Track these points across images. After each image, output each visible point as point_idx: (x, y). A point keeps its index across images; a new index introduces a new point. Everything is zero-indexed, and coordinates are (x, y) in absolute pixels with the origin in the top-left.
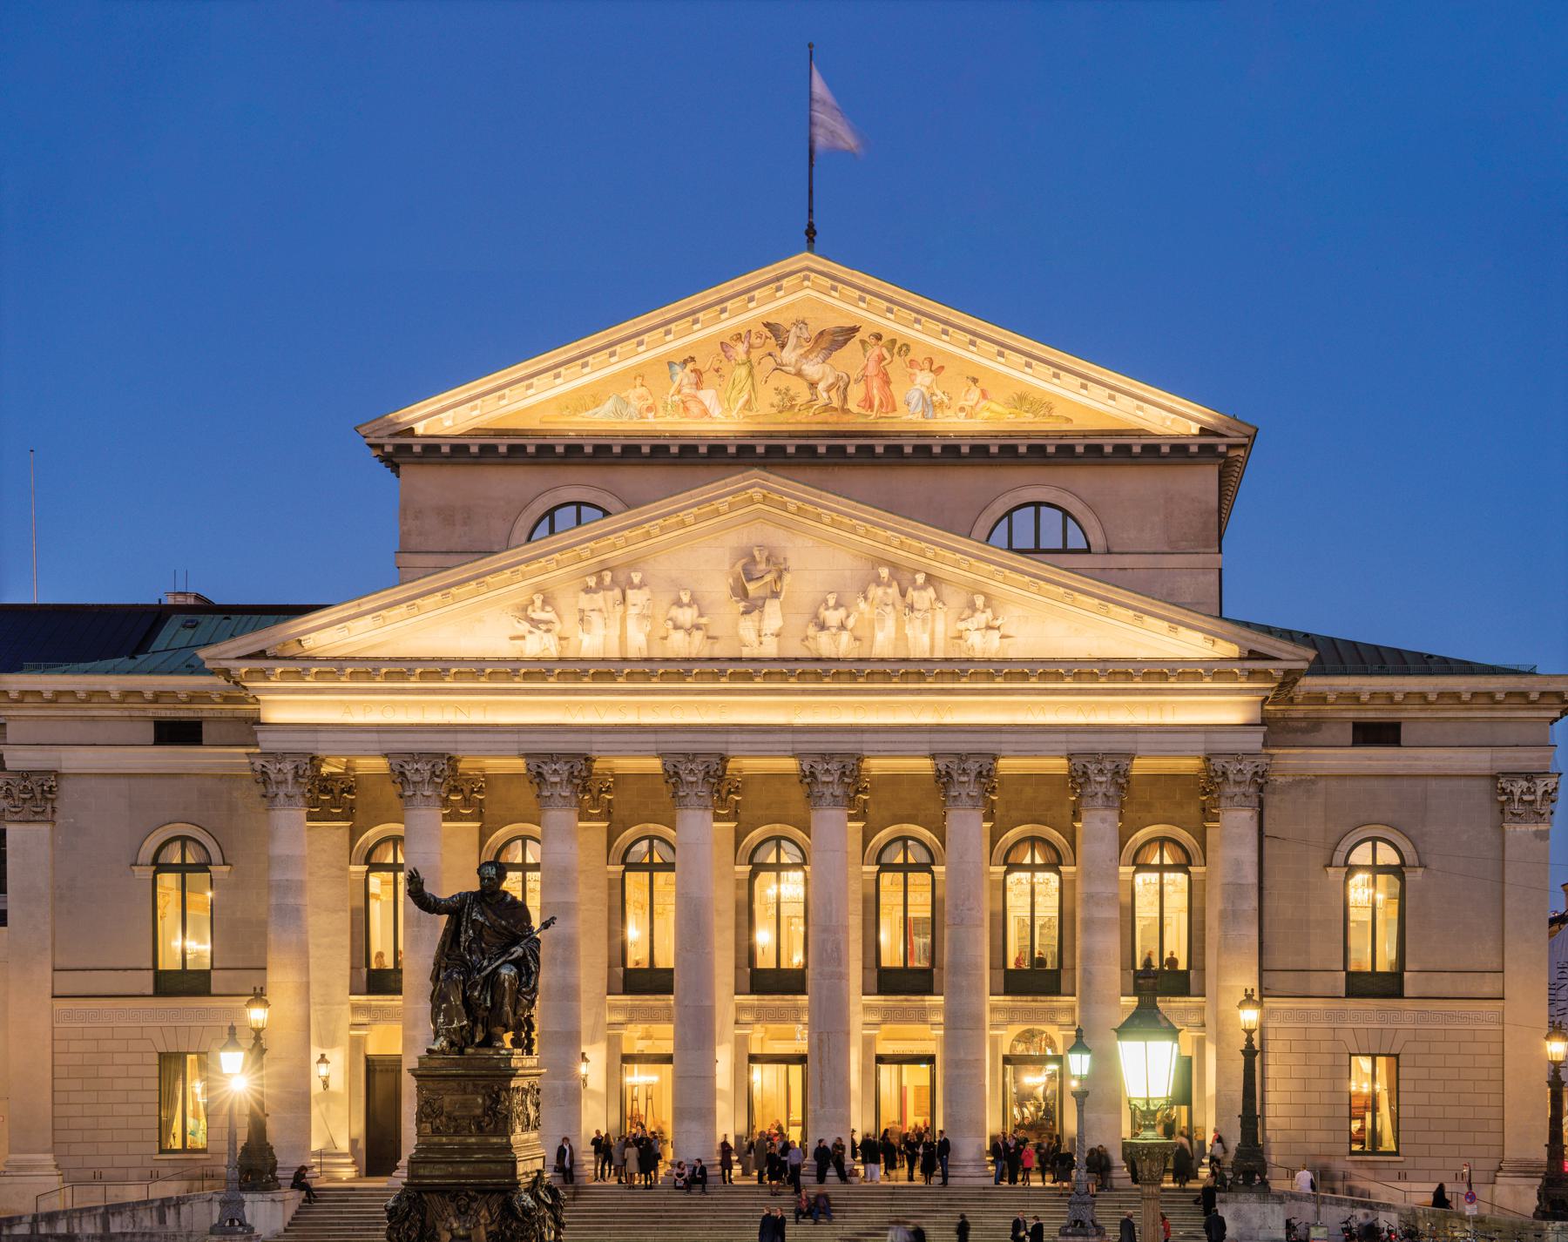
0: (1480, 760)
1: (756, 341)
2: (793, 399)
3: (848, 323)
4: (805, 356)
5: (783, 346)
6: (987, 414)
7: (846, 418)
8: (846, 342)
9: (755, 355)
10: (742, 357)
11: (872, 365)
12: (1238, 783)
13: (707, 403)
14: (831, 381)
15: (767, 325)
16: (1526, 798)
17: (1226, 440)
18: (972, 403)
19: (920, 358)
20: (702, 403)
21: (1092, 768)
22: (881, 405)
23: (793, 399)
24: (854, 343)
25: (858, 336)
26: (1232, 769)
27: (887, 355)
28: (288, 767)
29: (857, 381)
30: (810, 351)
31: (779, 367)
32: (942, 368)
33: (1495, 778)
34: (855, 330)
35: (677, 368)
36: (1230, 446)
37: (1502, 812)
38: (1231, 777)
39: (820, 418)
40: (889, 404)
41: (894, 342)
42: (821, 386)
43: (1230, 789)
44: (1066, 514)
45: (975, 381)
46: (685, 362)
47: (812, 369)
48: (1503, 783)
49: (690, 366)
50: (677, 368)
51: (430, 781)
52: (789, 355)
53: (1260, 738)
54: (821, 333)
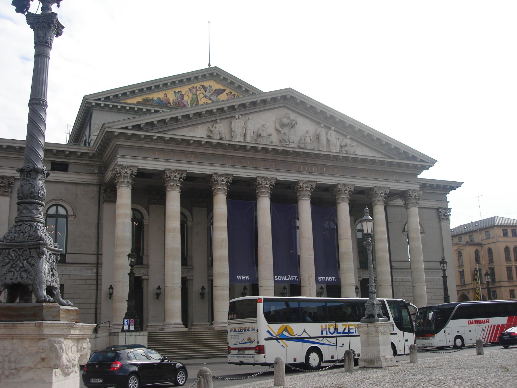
1: (198, 89)
3: (222, 88)
5: (206, 91)
8: (222, 93)
9: (198, 93)
15: (201, 85)
24: (224, 93)
25: (226, 92)
28: (129, 172)
30: (213, 94)
31: (205, 96)
33: (438, 209)
37: (439, 218)
46: (179, 92)
47: (213, 98)
52: (207, 94)
53: (419, 186)
54: (216, 90)
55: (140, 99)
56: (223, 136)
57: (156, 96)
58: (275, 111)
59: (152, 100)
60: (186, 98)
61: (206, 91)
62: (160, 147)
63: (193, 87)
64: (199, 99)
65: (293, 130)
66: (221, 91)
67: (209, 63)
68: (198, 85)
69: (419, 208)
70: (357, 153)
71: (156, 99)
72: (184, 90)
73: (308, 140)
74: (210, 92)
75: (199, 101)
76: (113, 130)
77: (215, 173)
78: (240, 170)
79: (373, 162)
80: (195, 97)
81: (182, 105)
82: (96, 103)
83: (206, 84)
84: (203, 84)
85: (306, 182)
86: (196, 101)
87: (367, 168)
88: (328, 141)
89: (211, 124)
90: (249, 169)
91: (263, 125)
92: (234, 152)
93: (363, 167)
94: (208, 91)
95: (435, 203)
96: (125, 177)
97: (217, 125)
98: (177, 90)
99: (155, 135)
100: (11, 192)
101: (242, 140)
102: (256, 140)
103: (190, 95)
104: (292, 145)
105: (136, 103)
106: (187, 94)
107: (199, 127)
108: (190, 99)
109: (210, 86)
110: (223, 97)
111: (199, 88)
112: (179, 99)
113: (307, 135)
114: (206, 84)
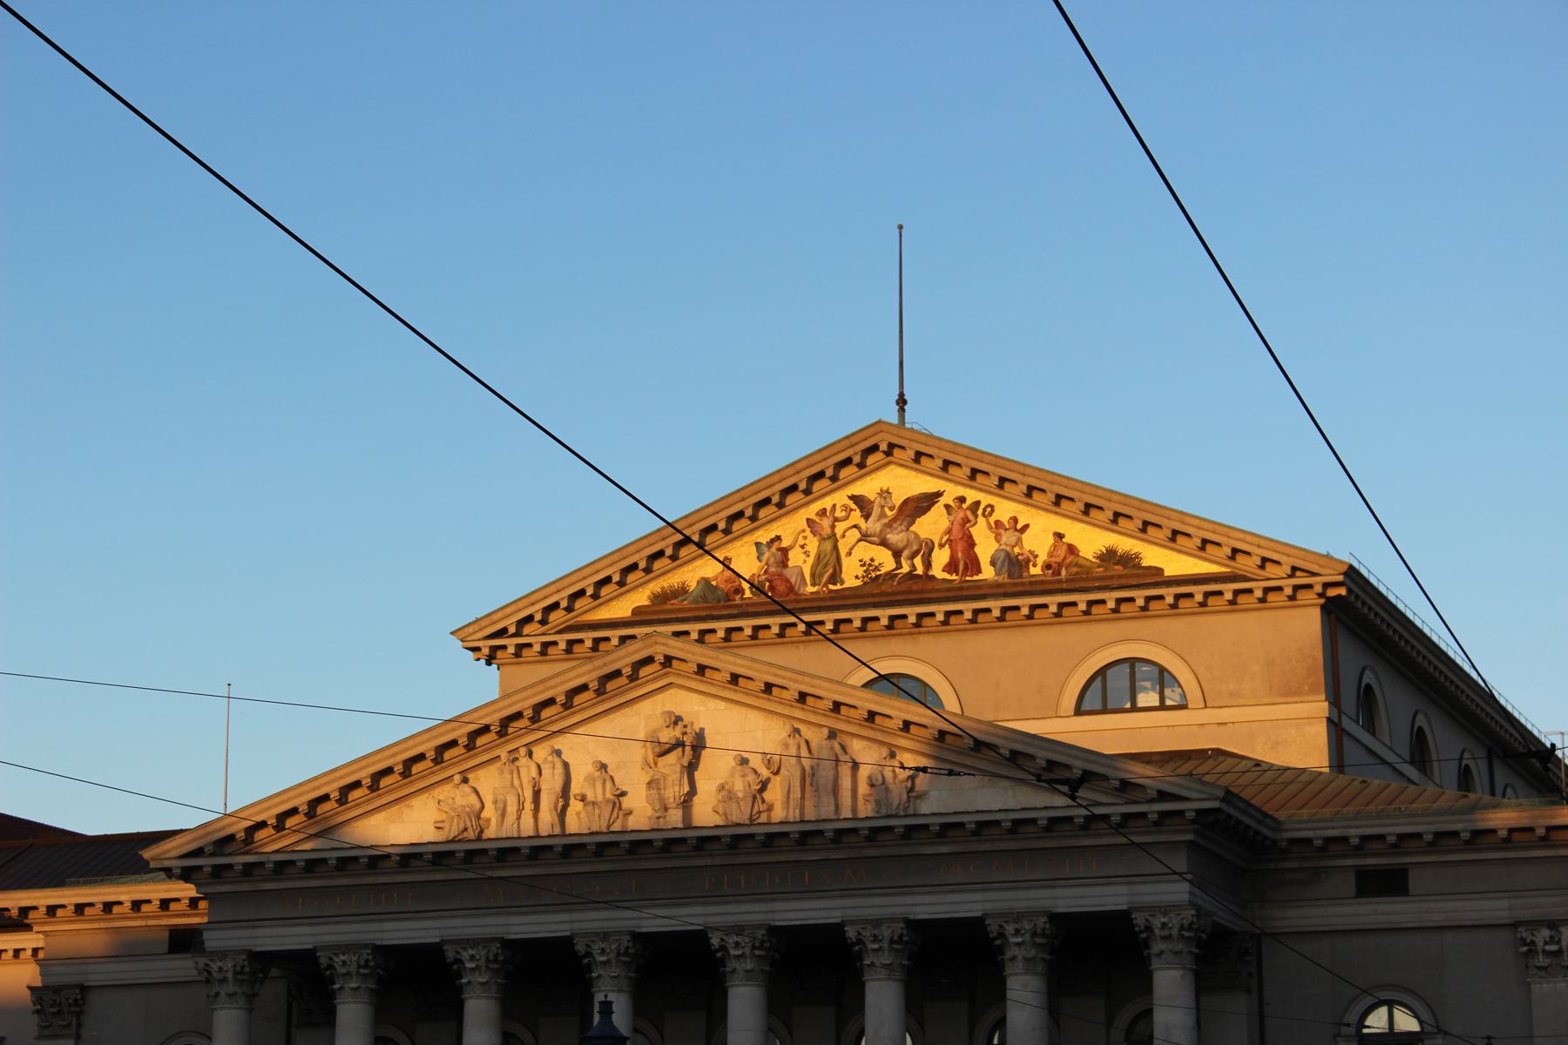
0: (1497, 909)
1: (839, 514)
2: (877, 569)
4: (889, 525)
6: (1075, 570)
7: (930, 585)
8: (929, 508)
10: (828, 531)
11: (956, 528)
13: (793, 581)
14: (915, 548)
15: (852, 498)
16: (1548, 948)
17: (1318, 579)
18: (1059, 560)
19: (1005, 520)
20: (788, 581)
21: (1010, 929)
22: (966, 568)
23: (877, 569)
24: (938, 509)
25: (943, 500)
26: (1157, 922)
27: (971, 517)
29: (941, 546)
30: (894, 520)
31: (865, 537)
32: (1026, 526)
33: (1515, 925)
34: (939, 494)
35: (765, 549)
36: (1326, 585)
38: (1157, 932)
39: (904, 587)
40: (974, 565)
41: (978, 503)
42: (906, 553)
43: (1156, 947)
44: (1162, 670)
45: (1059, 536)
46: (772, 541)
47: (895, 538)
48: (1523, 933)
49: (776, 544)
50: (765, 549)
51: (358, 974)
54: (906, 502)
55: (641, 598)
57: (698, 572)
58: (646, 705)
59: (682, 591)
60: (796, 558)
61: (867, 517)
63: (823, 512)
64: (843, 552)
66: (925, 503)
67: (901, 395)
68: (840, 498)
71: (693, 585)
72: (789, 527)
74: (883, 515)
75: (845, 561)
76: (167, 864)
78: (526, 919)
79: (949, 829)
80: (828, 546)
81: (781, 588)
82: (494, 649)
83: (868, 487)
84: (858, 489)
85: (738, 929)
86: (833, 561)
90: (555, 912)
93: (944, 849)
94: (876, 511)
95: (1504, 903)
96: (225, 980)
98: (763, 536)
100: (79, 1026)
101: (527, 827)
103: (813, 545)
105: (628, 613)
106: (801, 541)
107: (415, 802)
108: (811, 561)
109: (885, 494)
110: (932, 525)
111: (846, 508)
112: (772, 569)
114: (868, 487)
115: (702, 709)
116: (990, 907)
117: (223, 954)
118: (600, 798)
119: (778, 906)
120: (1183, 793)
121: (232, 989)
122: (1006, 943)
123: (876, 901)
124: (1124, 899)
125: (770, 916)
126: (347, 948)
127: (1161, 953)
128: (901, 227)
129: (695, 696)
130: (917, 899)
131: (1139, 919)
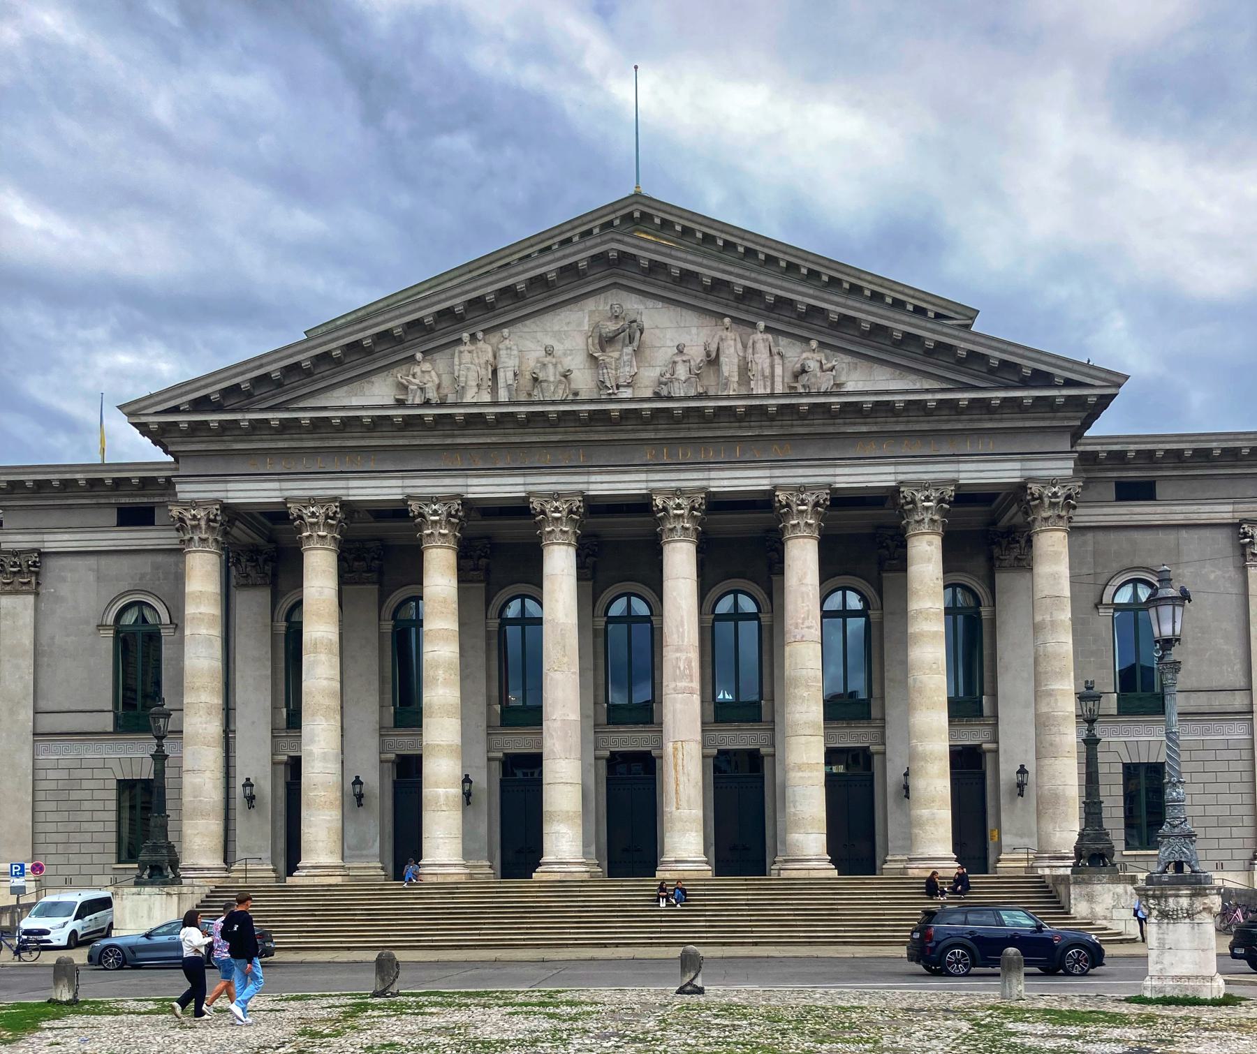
12: (1053, 505)
21: (919, 496)
26: (1047, 493)
38: (1046, 501)
53: (1071, 464)
56: (433, 395)
58: (590, 304)
62: (273, 445)
65: (629, 350)
69: (1075, 531)
70: (850, 387)
73: (682, 372)
77: (409, 497)
79: (884, 409)
85: (678, 493)
87: (874, 429)
88: (745, 370)
89: (405, 367)
91: (549, 352)
92: (463, 436)
93: (864, 429)
97: (417, 369)
99: (245, 417)
101: (487, 398)
102: (530, 395)
104: (626, 393)
107: (374, 379)
113: (678, 359)
115: (641, 307)
116: (901, 477)
117: (194, 504)
118: (552, 379)
119: (713, 474)
120: (1088, 380)
121: (204, 536)
122: (915, 508)
123: (800, 471)
124: (1018, 474)
125: (704, 483)
126: (312, 501)
127: (1046, 519)
128: (636, 67)
129: (634, 297)
130: (839, 471)
131: (1035, 488)
